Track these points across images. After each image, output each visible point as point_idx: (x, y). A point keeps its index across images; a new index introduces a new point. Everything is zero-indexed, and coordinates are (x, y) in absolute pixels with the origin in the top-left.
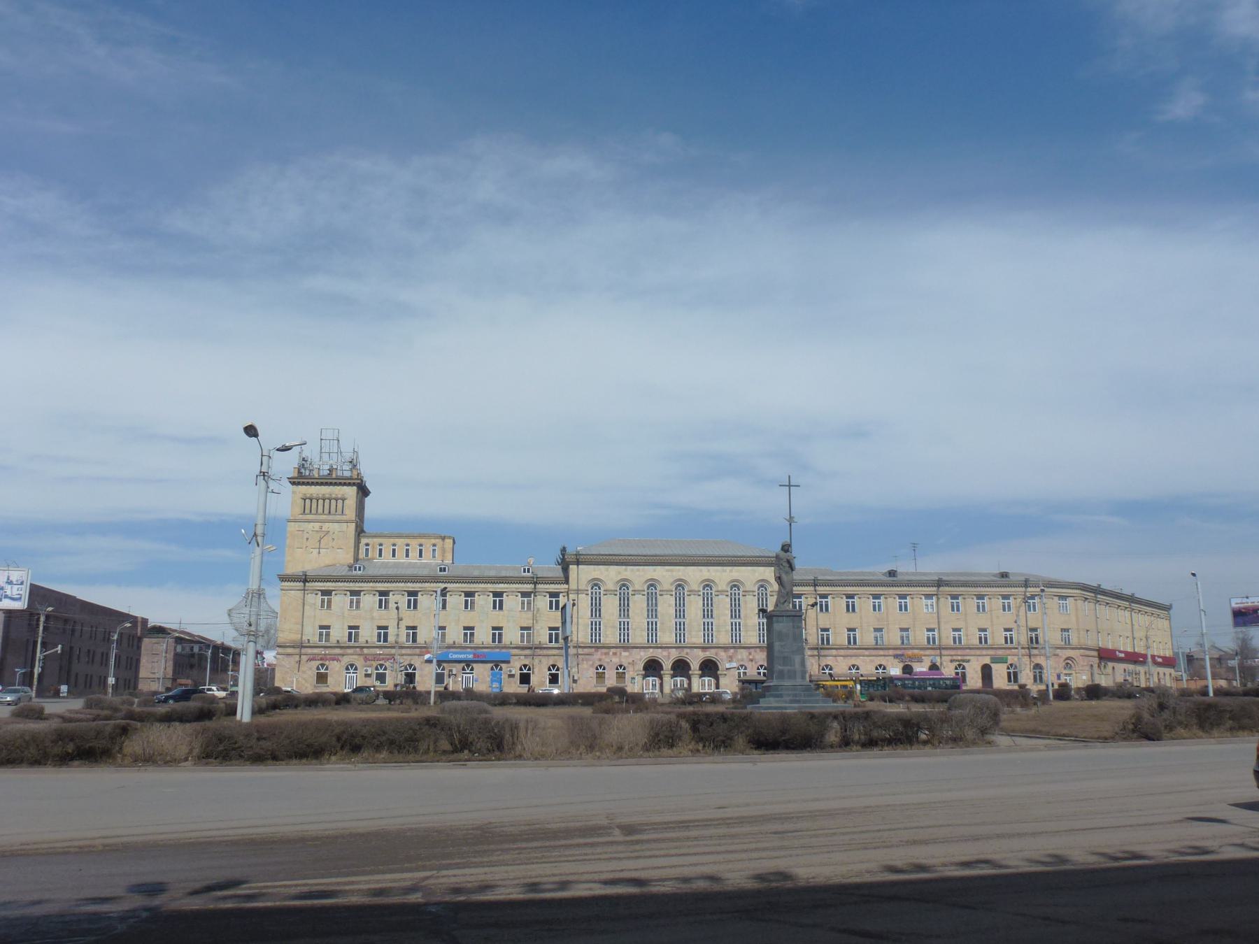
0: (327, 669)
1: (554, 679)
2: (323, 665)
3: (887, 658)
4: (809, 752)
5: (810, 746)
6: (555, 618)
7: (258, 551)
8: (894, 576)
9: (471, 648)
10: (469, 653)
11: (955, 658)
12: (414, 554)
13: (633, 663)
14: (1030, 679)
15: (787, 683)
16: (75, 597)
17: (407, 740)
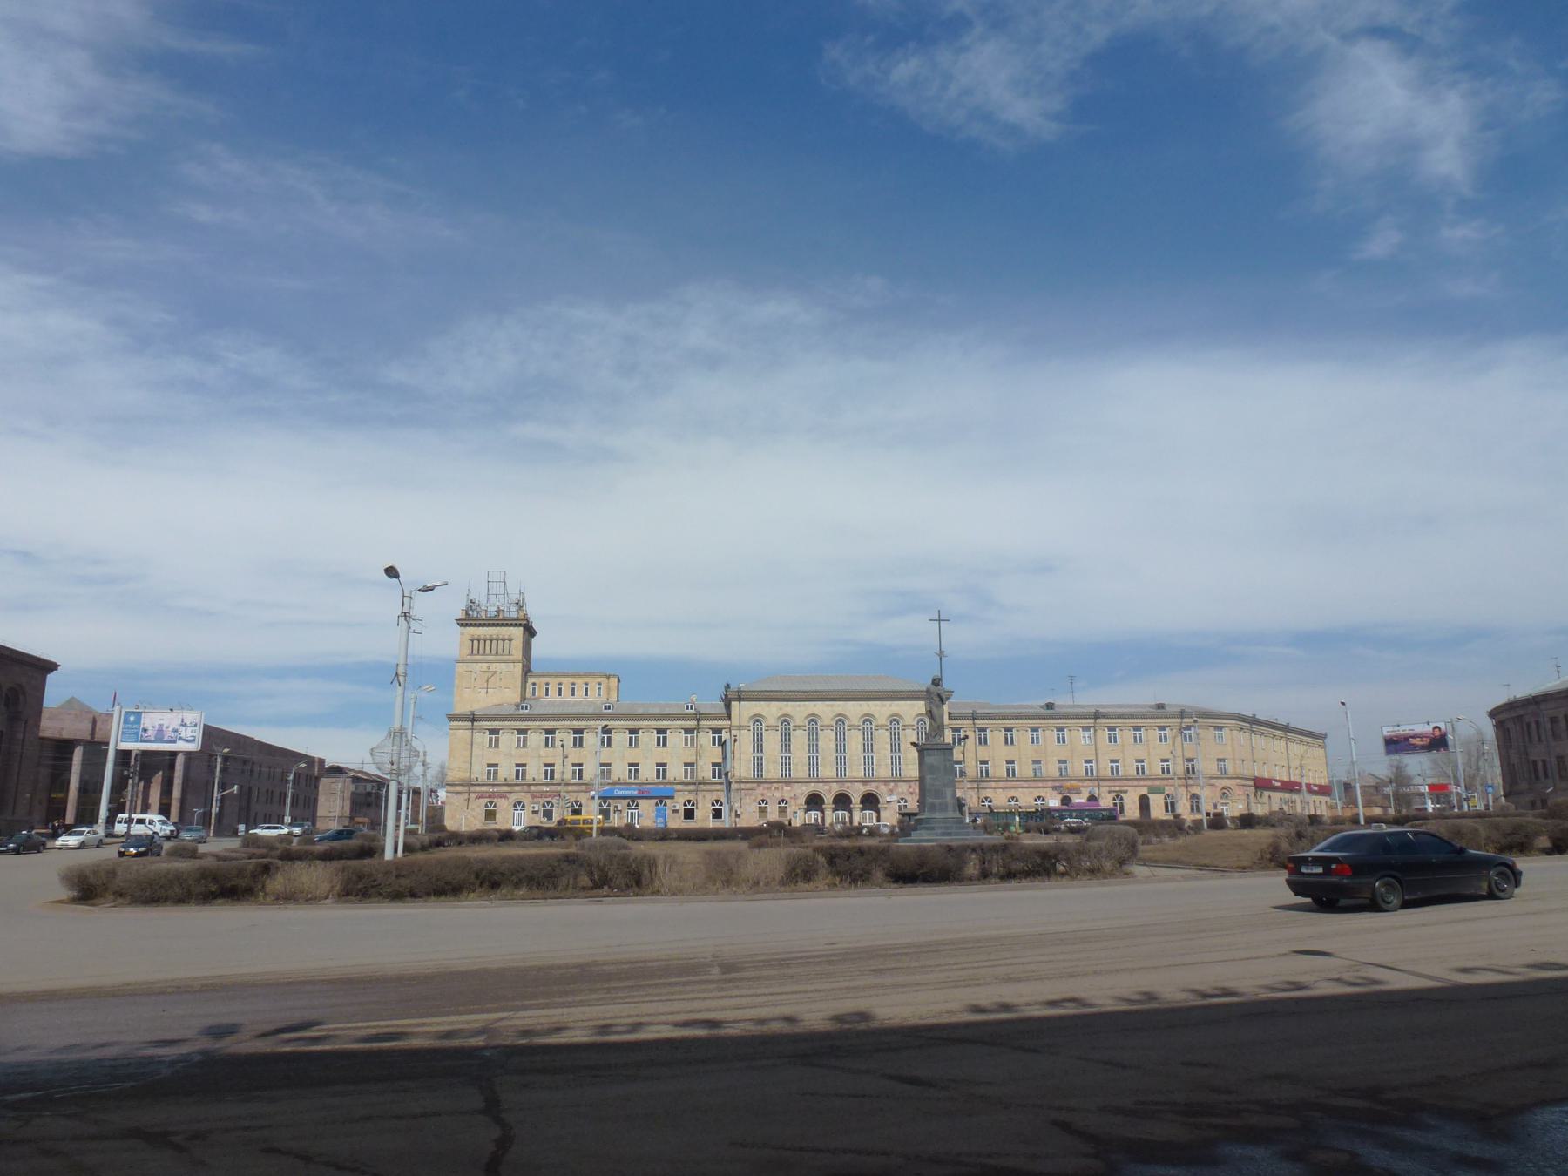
0: (495, 806)
1: (717, 814)
2: (491, 803)
3: (1045, 790)
4: (946, 885)
5: (948, 879)
6: (715, 754)
7: (400, 690)
9: (636, 784)
11: (1113, 789)
12: (580, 692)
13: (795, 798)
15: (938, 815)
16: (253, 739)
17: (545, 876)
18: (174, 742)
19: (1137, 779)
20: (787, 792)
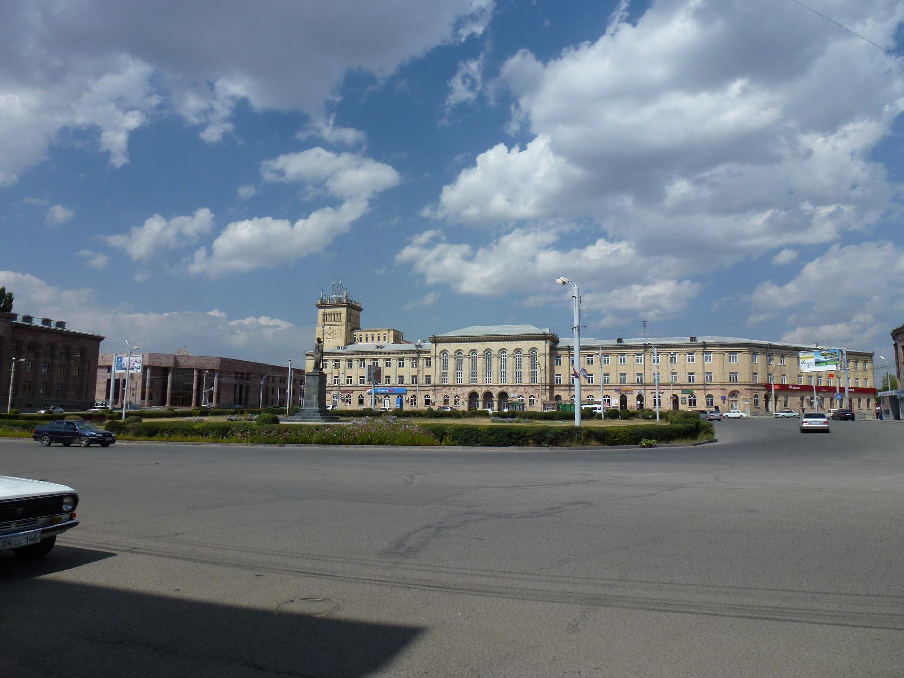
1: (427, 402)
3: (611, 391)
8: (695, 340)
10: (387, 389)
12: (376, 339)
13: (463, 394)
14: (704, 404)
18: (133, 369)
19: (587, 386)
20: (459, 391)
